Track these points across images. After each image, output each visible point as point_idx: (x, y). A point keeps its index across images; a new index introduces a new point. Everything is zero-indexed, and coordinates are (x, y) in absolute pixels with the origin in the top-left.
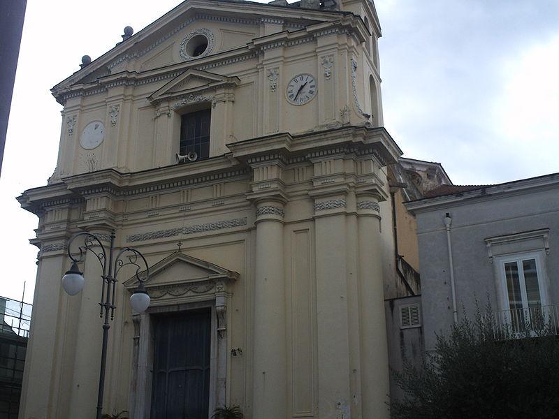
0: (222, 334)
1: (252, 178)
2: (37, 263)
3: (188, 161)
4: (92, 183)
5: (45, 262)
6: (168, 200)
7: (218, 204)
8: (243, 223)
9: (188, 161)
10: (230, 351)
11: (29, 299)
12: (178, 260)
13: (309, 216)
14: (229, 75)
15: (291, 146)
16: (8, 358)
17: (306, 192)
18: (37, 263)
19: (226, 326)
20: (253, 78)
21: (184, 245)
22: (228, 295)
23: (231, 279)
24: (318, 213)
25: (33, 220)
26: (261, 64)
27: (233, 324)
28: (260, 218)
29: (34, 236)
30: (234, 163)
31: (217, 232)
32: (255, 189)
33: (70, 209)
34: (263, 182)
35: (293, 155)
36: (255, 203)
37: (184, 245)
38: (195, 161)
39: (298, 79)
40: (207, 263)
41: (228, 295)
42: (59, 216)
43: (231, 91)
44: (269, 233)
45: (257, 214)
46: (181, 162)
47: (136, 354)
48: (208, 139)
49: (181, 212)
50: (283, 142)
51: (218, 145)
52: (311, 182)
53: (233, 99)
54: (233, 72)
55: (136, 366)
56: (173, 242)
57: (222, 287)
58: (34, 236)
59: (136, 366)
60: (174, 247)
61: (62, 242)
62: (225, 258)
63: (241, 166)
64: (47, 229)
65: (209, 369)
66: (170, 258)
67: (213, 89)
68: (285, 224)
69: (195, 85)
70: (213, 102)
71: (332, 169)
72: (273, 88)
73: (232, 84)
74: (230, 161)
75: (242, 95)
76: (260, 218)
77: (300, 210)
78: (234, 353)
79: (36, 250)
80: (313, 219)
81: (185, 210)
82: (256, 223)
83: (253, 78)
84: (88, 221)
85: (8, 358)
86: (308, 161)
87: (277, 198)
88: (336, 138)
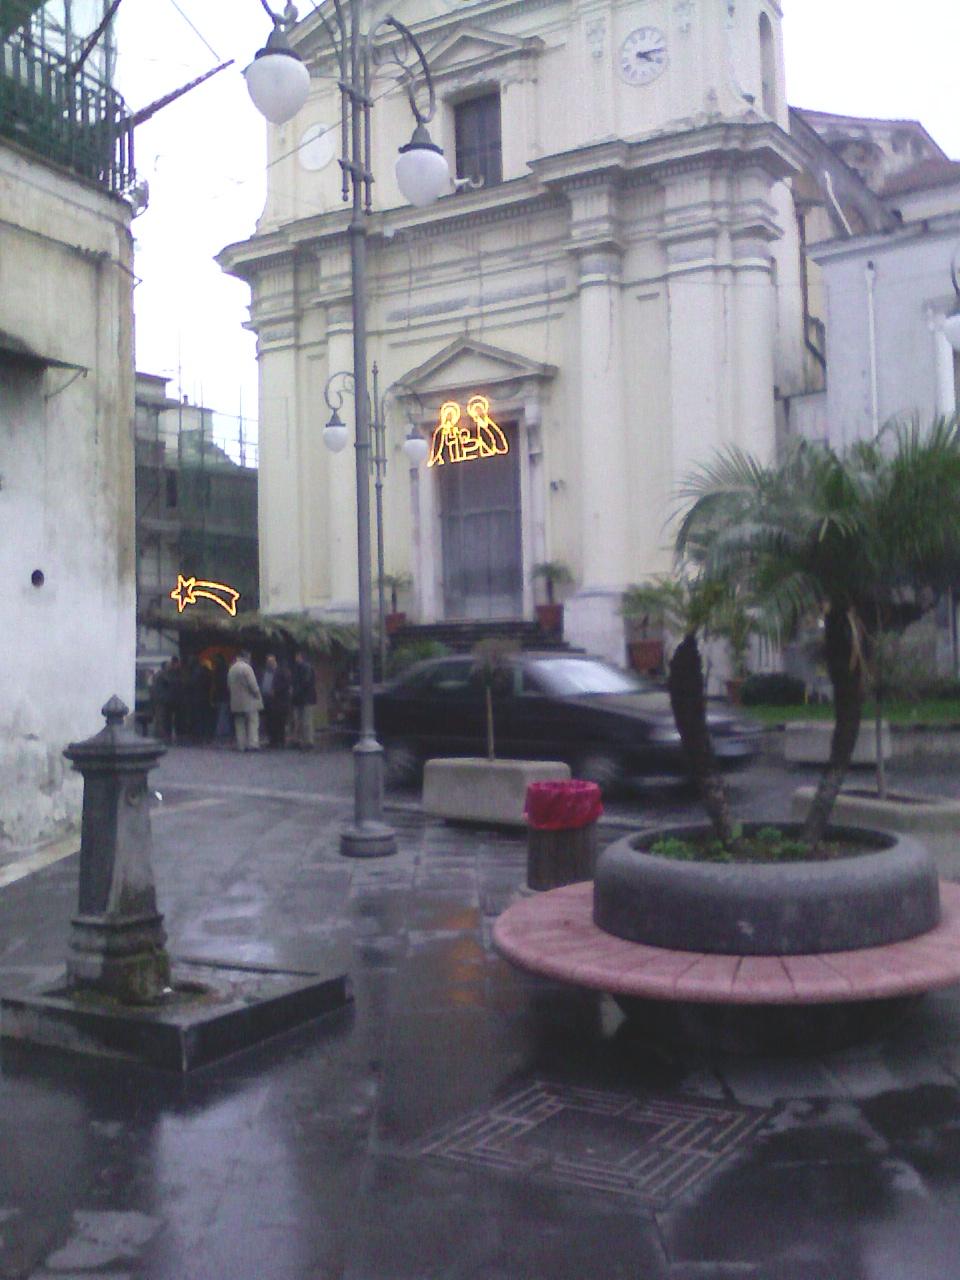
0: (597, 54)
1: (569, 214)
2: (257, 358)
3: (471, 190)
4: (324, 232)
5: (268, 358)
6: (444, 253)
7: (522, 256)
8: (560, 284)
9: (471, 190)
10: (548, 486)
11: (252, 412)
12: (464, 349)
13: (658, 272)
14: (525, 32)
15: (628, 160)
16: (394, 53)
17: (653, 233)
18: (257, 358)
19: (541, 447)
20: (563, 38)
21: (475, 324)
22: (543, 400)
23: (546, 377)
24: (674, 268)
25: (241, 290)
26: (576, 12)
27: (548, 443)
28: (585, 279)
29: (247, 317)
30: (541, 190)
31: (523, 301)
32: (576, 233)
33: (296, 273)
34: (589, 222)
35: (631, 177)
36: (577, 254)
37: (475, 324)
38: (479, 189)
39: (637, 37)
40: (510, 354)
41: (543, 400)
42: (279, 285)
43: (530, 62)
44: (595, 302)
45: (581, 272)
46: (460, 191)
47: (415, 493)
48: (497, 146)
49: (466, 270)
50: (613, 155)
51: (514, 162)
52: (661, 217)
53: (533, 76)
54: (530, 26)
55: (416, 510)
56: (456, 320)
57: (532, 389)
58: (247, 317)
59: (416, 510)
60: (459, 328)
61: (290, 326)
62: (531, 345)
63: (556, 198)
64: (265, 306)
65: (518, 512)
66: (453, 346)
67: (501, 61)
68: (622, 287)
69: (471, 54)
70: (502, 85)
71: (692, 197)
72: (598, 55)
73: (531, 50)
74: (533, 188)
75: (549, 65)
76: (585, 279)
77: (643, 263)
78: (554, 486)
79: (253, 337)
80: (665, 278)
81: (474, 267)
82: (581, 287)
83: (563, 38)
84: (325, 292)
85: (394, 53)
86: (655, 182)
87: (608, 248)
88: (698, 144)
